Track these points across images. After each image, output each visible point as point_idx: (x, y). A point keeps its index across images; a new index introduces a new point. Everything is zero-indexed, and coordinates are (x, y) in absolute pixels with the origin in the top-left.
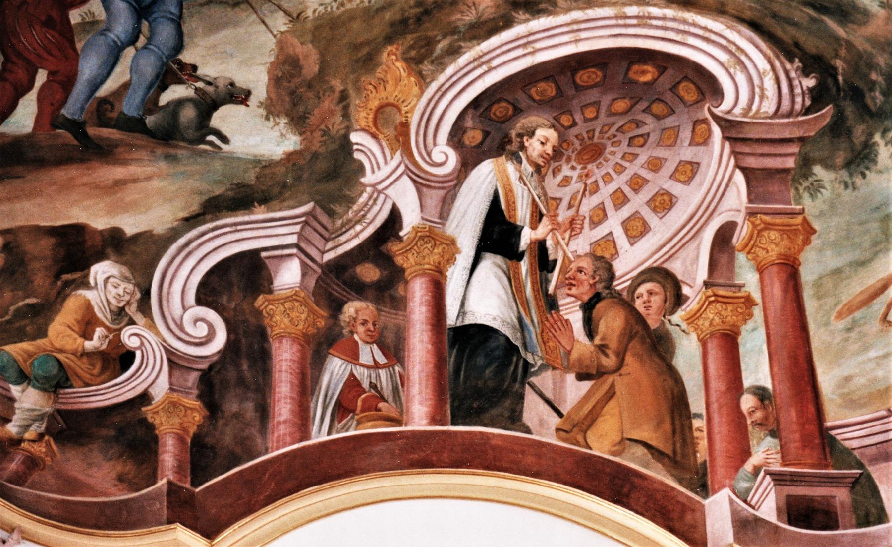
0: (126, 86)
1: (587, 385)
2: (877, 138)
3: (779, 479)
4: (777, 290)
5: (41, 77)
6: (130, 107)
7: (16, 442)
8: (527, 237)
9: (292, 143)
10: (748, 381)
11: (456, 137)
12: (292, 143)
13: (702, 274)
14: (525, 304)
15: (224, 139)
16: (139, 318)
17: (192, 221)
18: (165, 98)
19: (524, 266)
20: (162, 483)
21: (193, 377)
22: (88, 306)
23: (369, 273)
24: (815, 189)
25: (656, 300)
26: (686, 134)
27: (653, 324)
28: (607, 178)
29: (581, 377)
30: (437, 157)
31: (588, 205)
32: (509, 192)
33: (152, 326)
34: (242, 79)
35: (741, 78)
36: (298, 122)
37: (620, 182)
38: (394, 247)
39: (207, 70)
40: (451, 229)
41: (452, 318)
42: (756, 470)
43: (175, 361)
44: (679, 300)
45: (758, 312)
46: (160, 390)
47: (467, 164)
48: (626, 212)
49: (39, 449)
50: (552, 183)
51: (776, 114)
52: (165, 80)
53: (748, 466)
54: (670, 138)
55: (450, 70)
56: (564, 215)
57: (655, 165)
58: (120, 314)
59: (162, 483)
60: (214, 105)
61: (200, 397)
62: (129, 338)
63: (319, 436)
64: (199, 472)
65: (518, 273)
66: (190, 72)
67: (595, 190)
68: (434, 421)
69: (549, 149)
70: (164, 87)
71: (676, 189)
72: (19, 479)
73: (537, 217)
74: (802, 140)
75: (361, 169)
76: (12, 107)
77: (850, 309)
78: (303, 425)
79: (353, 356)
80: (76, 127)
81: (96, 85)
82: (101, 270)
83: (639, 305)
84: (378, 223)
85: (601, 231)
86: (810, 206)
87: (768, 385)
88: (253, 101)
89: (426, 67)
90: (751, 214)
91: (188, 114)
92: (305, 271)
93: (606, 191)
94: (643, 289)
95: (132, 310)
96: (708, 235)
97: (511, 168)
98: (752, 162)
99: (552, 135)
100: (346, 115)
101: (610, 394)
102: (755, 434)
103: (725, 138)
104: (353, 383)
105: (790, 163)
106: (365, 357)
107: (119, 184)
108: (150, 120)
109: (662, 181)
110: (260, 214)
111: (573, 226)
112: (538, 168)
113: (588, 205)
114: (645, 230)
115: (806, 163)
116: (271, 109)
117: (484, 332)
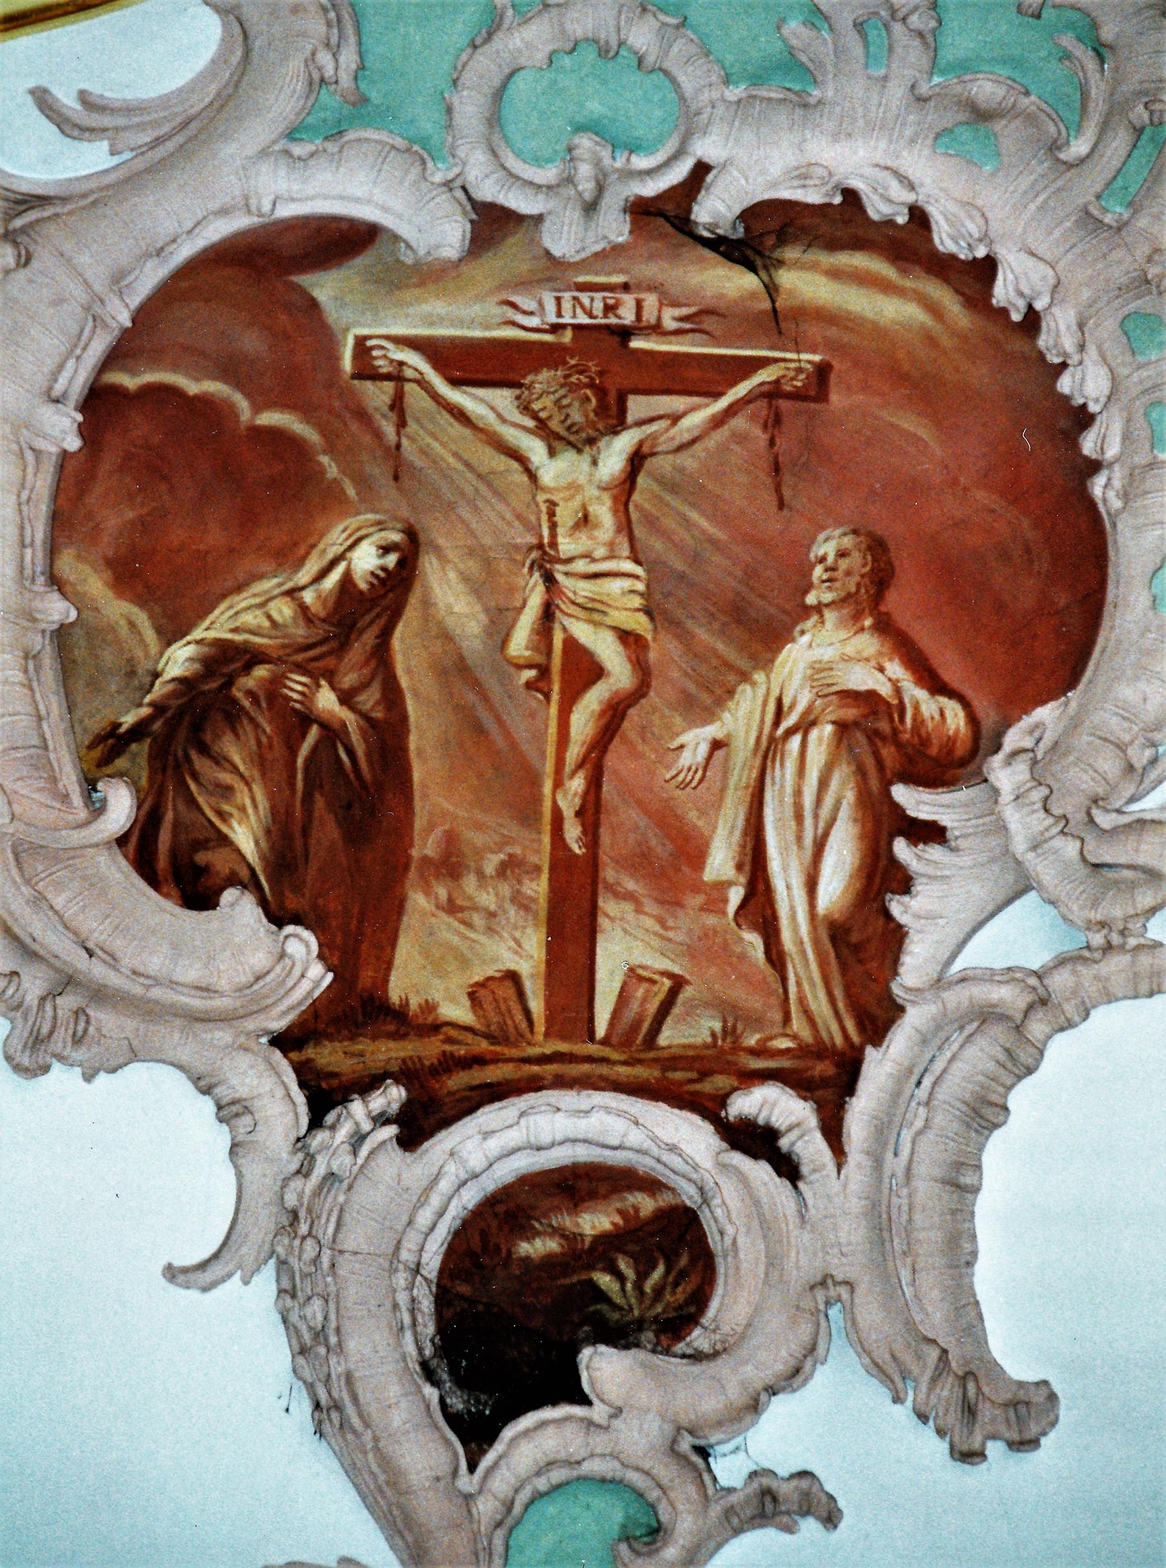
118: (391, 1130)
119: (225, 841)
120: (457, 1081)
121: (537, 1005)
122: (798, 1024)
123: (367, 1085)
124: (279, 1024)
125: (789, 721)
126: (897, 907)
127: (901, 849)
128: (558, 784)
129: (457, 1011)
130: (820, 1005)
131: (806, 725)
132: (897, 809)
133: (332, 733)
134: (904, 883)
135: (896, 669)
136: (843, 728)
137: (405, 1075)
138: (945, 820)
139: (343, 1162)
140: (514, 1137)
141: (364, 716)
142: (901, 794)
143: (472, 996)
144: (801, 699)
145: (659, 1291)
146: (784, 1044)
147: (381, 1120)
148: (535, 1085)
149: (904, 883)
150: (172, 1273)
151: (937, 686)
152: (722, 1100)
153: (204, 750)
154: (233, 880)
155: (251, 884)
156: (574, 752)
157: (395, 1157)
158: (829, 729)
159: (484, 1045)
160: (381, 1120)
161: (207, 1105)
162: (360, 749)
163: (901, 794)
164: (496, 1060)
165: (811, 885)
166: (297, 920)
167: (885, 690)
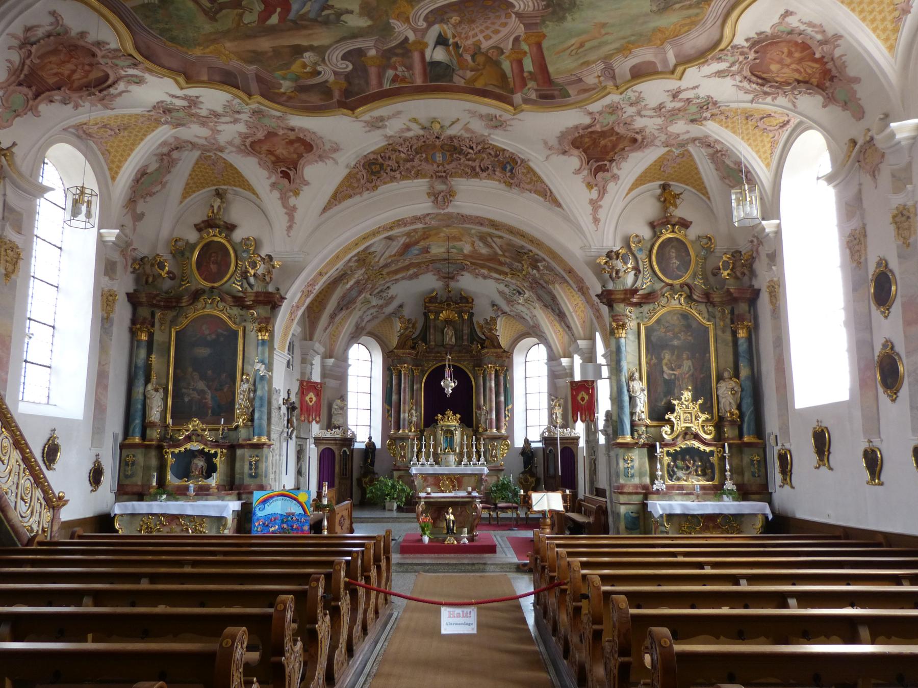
0: (309, 11)
1: (473, 73)
2: (567, 15)
3: (536, 90)
4: (535, 49)
5: (279, 10)
6: (312, 15)
7: (284, 93)
8: (451, 41)
9: (369, 23)
10: (526, 69)
11: (426, 19)
12: (369, 23)
13: (510, 46)
14: (452, 56)
15: (346, 23)
16: (322, 64)
17: (337, 42)
18: (324, 13)
19: (451, 48)
20: (335, 100)
21: (342, 77)
22: (304, 62)
23: (399, 51)
24: (547, 26)
25: (495, 54)
26: (503, 16)
27: (494, 59)
28: (477, 27)
29: (471, 71)
30: (419, 24)
31: (471, 34)
32: (445, 31)
33: (327, 65)
34: (350, 8)
35: (521, 3)
36: (371, 17)
37: (482, 28)
38: (406, 45)
39: (337, 6)
40: (426, 40)
41: (428, 58)
42: (529, 89)
43: (335, 73)
44: (502, 53)
45: (529, 55)
46: (332, 78)
47: (430, 25)
48: (484, 34)
49: (293, 95)
50: (459, 29)
51: (533, 10)
52: (323, 8)
53: (527, 88)
54: (499, 17)
55: (422, 4)
56: (463, 36)
57: (493, 23)
58: (316, 64)
59: (335, 100)
60: (341, 15)
61: (346, 80)
62: (319, 68)
63: (387, 86)
64: (347, 98)
65: (449, 51)
66: (332, 7)
67: (474, 29)
68: (424, 82)
69: (457, 21)
70: (323, 11)
71: (500, 29)
72: (287, 101)
73: (454, 37)
74: (542, 16)
75: (394, 28)
76: (269, 17)
77: (558, 53)
78: (380, 84)
79: (395, 69)
80: (294, 22)
81: (298, 11)
82: (307, 55)
83: (489, 55)
84: (401, 40)
85: (477, 38)
86: (544, 30)
87: (533, 70)
88: (354, 13)
89: (414, 3)
90: (525, 33)
91: (332, 17)
92: (377, 52)
93: (477, 30)
94: (491, 51)
95: (320, 63)
96: (511, 39)
97: (445, 26)
98: (526, 22)
99: (458, 19)
100: (387, 15)
101: (482, 74)
102: (528, 82)
103: (516, 17)
104: (396, 75)
105: (538, 21)
106: (400, 69)
107: (310, 35)
108: (319, 19)
109: (496, 27)
110: (360, 39)
111: (467, 38)
112: (454, 26)
113: (471, 34)
114: (491, 38)
115: (543, 22)
116: (361, 14)
117: (438, 63)
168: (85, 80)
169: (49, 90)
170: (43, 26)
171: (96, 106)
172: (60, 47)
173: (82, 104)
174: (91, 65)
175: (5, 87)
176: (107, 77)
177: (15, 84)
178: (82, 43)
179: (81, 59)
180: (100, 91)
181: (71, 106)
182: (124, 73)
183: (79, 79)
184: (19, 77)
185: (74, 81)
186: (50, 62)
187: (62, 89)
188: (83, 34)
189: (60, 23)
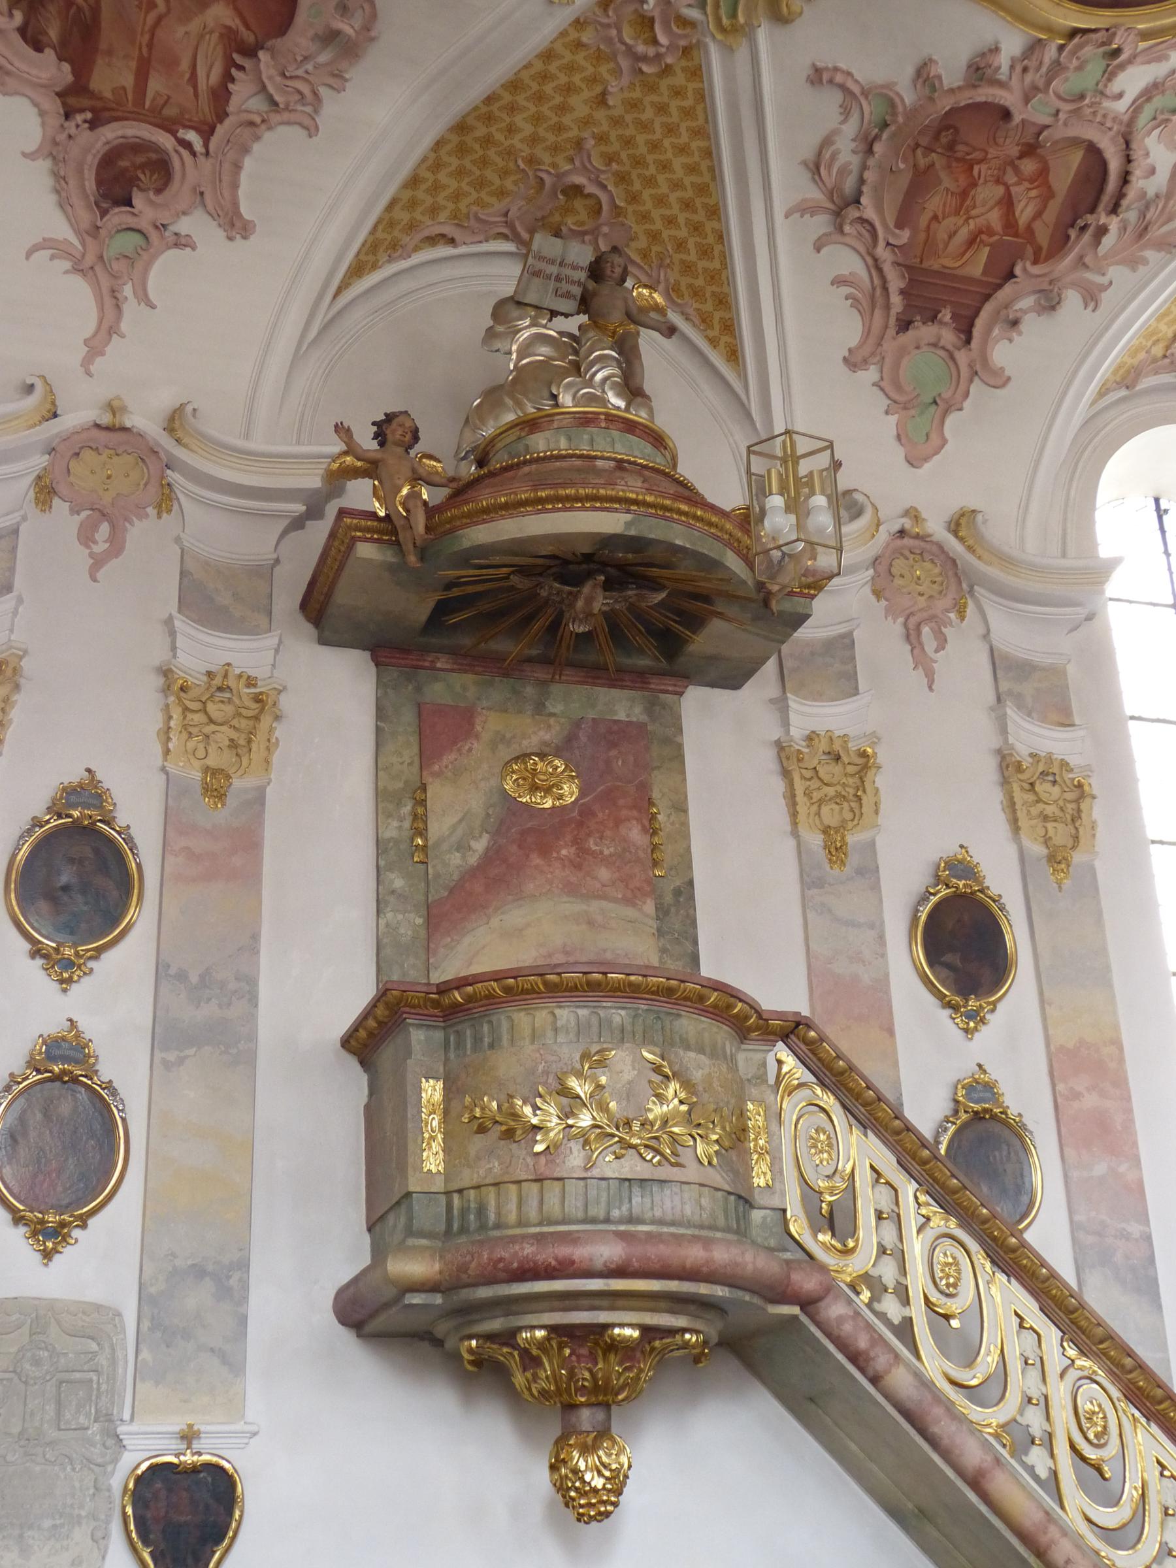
118: (87, 125)
119: (47, 34)
120: (107, 114)
121: (130, 98)
122: (200, 114)
123: (82, 111)
124: (57, 89)
125: (207, 30)
126: (231, 86)
127: (234, 71)
128: (142, 34)
129: (108, 94)
130: (207, 110)
131: (211, 32)
132: (233, 60)
133: (79, 9)
134: (233, 80)
135: (238, 21)
136: (221, 35)
137: (92, 110)
138: (245, 65)
139: (73, 131)
140: (120, 133)
141: (89, 5)
142: (235, 56)
143: (113, 91)
144: (211, 24)
145: (156, 180)
146: (196, 119)
147: (85, 121)
148: (127, 119)
149: (233, 80)
150: (24, 155)
151: (248, 27)
152: (177, 132)
153: (43, 6)
154: (49, 46)
155: (54, 48)
156: (146, 29)
157: (88, 133)
158: (217, 34)
159: (114, 106)
160: (85, 121)
161: (35, 110)
162: (87, 13)
163: (235, 56)
164: (117, 110)
165: (208, 76)
166: (66, 60)
167: (234, 27)
168: (1054, 207)
169: (987, 297)
170: (835, 132)
171: (1145, 261)
172: (923, 162)
173: (1104, 280)
174: (1030, 150)
175: (873, 354)
176: (1093, 151)
177: (891, 331)
178: (945, 104)
179: (992, 152)
180: (1114, 209)
181: (1072, 299)
182: (1122, 106)
183: (1038, 215)
184: (887, 307)
185: (1029, 229)
186: (935, 217)
187: (1018, 270)
188: (924, 75)
189: (856, 90)
